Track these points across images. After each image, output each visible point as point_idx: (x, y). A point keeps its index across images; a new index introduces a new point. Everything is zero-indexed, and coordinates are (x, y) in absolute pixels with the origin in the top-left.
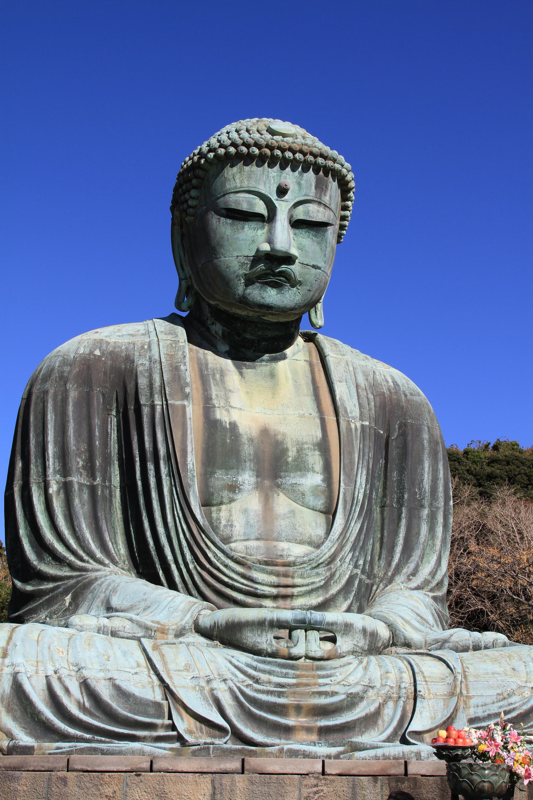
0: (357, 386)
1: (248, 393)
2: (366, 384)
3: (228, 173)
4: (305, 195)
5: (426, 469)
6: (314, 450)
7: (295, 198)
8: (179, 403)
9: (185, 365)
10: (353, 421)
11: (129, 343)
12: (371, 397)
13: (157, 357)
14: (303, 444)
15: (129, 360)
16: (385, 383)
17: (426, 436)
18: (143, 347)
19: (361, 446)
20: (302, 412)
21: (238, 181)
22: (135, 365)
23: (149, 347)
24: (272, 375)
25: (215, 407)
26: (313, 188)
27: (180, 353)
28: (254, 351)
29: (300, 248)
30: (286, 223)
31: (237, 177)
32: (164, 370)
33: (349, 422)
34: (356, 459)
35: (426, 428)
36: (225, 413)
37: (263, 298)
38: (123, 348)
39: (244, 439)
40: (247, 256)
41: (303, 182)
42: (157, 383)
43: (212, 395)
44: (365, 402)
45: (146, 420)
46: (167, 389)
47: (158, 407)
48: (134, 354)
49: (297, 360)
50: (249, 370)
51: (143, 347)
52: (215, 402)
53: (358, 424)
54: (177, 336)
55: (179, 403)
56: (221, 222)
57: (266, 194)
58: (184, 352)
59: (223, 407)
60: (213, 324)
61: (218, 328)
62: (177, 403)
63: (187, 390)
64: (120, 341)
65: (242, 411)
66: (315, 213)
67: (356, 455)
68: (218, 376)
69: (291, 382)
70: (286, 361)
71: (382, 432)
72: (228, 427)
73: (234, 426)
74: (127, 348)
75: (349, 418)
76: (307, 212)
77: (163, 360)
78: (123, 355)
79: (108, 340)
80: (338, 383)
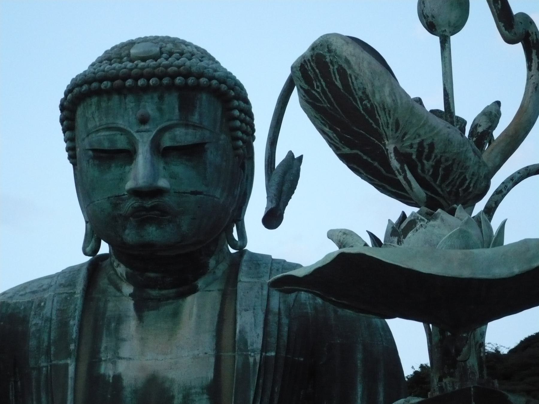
0: (267, 312)
1: (142, 339)
2: (282, 307)
3: (88, 112)
4: (168, 120)
5: (359, 393)
6: (203, 393)
7: (157, 126)
8: (62, 362)
9: (74, 319)
10: (252, 354)
11: (29, 302)
12: (285, 321)
13: (49, 315)
14: (190, 389)
15: (25, 320)
16: (311, 302)
17: (359, 356)
18: (39, 305)
19: (261, 381)
20: (196, 352)
21: (97, 119)
22: (30, 325)
23: (45, 304)
24: (176, 315)
25: (100, 360)
26: (177, 111)
27: (73, 306)
28: (160, 289)
29: (172, 177)
30: (149, 156)
31: (96, 114)
32: (53, 328)
33: (247, 357)
34: (252, 398)
35: (360, 347)
36: (110, 365)
37: (142, 237)
38: (22, 308)
39: (127, 393)
40: (119, 196)
41: (164, 107)
42: (46, 344)
43: (101, 348)
44: (273, 328)
45: (34, 384)
46: (53, 349)
47: (44, 369)
48: (30, 315)
49: (210, 291)
50: (151, 312)
51: (39, 305)
52: (103, 356)
53: (258, 357)
54: (75, 286)
55: (62, 362)
56: (90, 164)
57: (125, 128)
58: (76, 305)
59: (109, 359)
60: (118, 265)
61: (122, 270)
62: (61, 362)
63: (72, 347)
64: (21, 301)
65: (131, 362)
66: (183, 136)
67: (252, 393)
68: (113, 325)
69: (194, 317)
70: (197, 294)
71: (302, 359)
72: (111, 381)
73: (118, 378)
74: (25, 308)
75: (248, 351)
76: (174, 138)
77: (54, 317)
78: (21, 316)
79: (9, 301)
80: (244, 313)
